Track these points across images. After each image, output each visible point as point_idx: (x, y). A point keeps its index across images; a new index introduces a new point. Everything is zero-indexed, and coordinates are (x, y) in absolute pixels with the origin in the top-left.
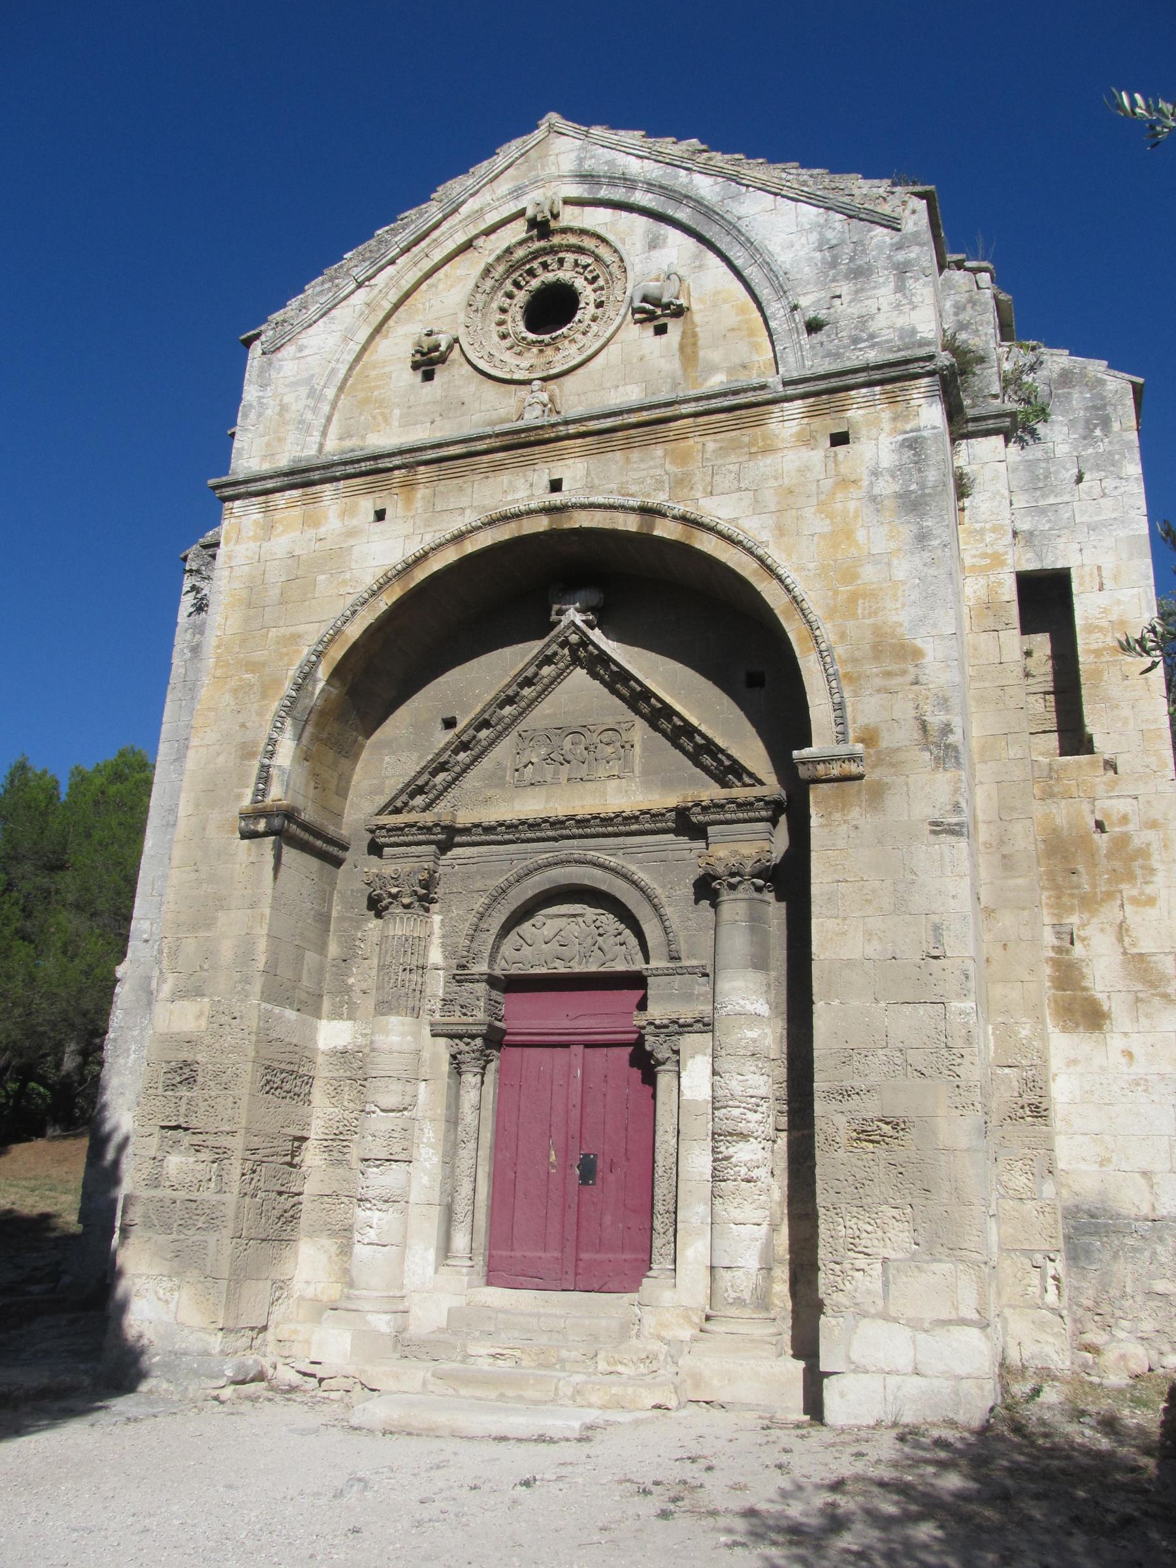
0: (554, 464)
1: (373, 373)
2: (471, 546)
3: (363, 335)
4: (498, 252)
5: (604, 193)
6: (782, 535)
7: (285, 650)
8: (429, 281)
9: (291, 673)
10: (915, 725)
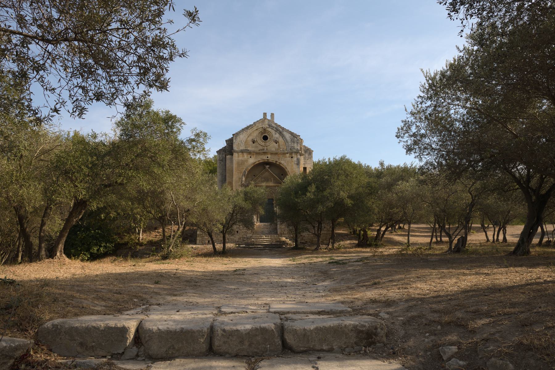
3: (247, 137)
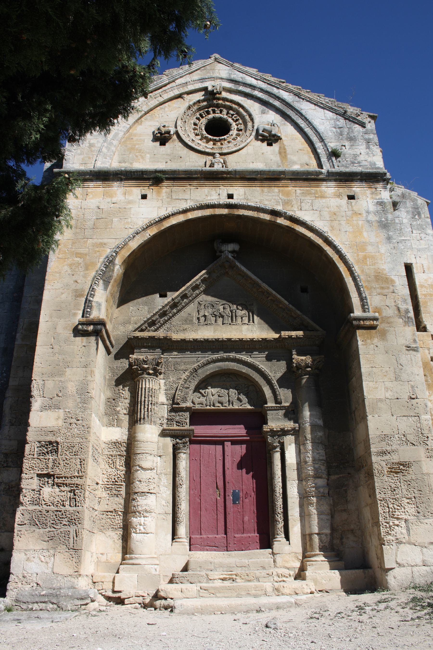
0: (229, 188)
1: (135, 138)
2: (191, 216)
4: (195, 101)
5: (241, 88)
6: (333, 230)
7: (97, 249)
8: (161, 106)
9: (101, 260)
10: (396, 308)
